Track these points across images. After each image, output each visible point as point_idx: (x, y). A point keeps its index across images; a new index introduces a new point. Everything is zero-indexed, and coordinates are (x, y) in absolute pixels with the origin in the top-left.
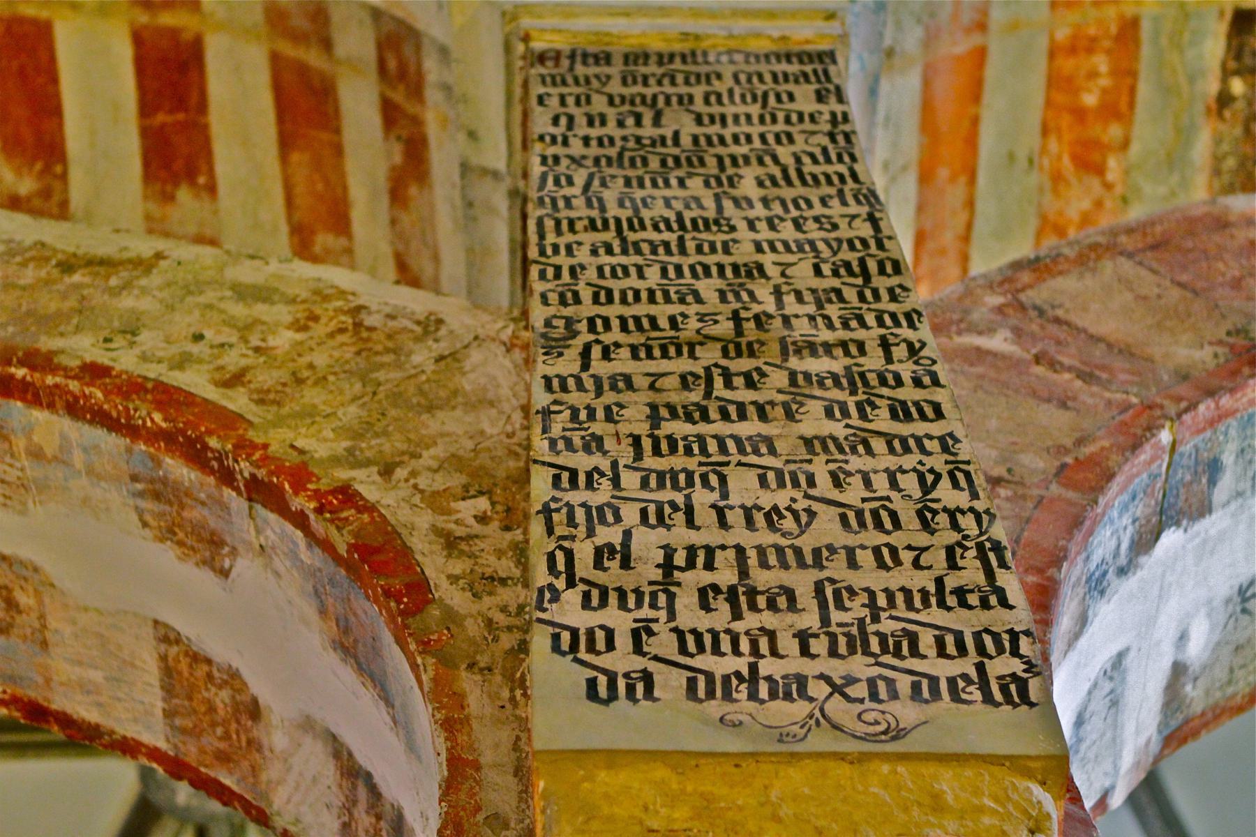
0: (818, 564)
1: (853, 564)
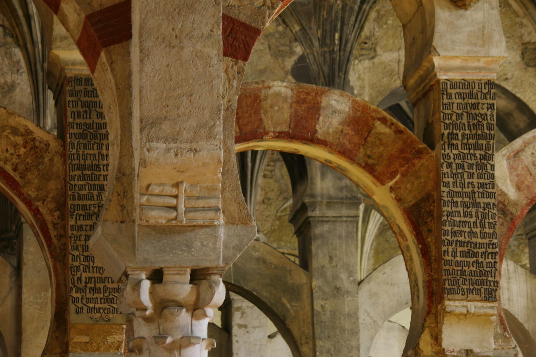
1: (108, 282)
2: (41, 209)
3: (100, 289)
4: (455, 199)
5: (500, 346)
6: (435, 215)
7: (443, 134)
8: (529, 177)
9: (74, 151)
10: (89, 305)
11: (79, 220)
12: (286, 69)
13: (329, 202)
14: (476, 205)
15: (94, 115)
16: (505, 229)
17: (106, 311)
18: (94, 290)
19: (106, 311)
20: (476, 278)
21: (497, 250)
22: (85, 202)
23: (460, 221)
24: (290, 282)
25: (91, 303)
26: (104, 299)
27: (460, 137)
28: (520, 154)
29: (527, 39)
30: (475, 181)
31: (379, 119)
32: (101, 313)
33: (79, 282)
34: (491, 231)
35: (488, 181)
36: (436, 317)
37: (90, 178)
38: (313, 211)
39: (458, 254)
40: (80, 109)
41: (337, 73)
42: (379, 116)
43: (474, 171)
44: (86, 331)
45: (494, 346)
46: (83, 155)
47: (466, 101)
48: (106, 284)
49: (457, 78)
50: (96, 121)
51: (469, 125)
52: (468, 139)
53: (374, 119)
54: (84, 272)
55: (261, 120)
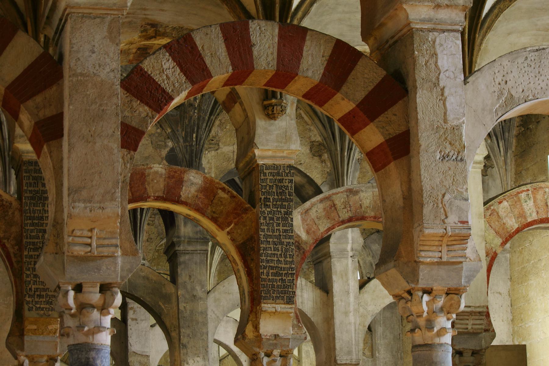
2: (6, 244)
3: (43, 295)
4: (268, 240)
5: (296, 332)
6: (256, 250)
7: (261, 198)
8: (314, 226)
9: (28, 208)
11: (31, 251)
12: (162, 156)
13: (189, 241)
14: (282, 243)
15: (40, 185)
16: (299, 259)
17: (47, 310)
18: (40, 296)
19: (47, 310)
20: (281, 289)
21: (294, 272)
22: (34, 240)
23: (271, 254)
24: (164, 291)
27: (271, 201)
28: (309, 211)
29: (313, 139)
30: (281, 228)
31: (221, 189)
34: (291, 260)
35: (289, 228)
36: (256, 314)
37: (37, 225)
38: (179, 247)
39: (270, 274)
40: (31, 181)
41: (194, 159)
42: (220, 187)
43: (280, 222)
44: (34, 323)
45: (292, 332)
46: (33, 210)
47: (275, 177)
48: (47, 292)
49: (270, 163)
50: (41, 189)
51: (277, 193)
52: (276, 202)
53: (217, 189)
55: (146, 189)
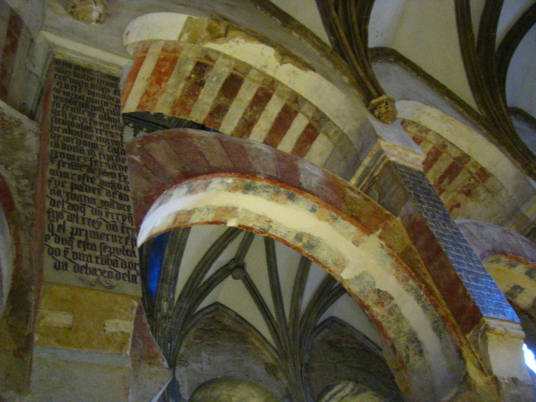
0: (101, 239)
1: (108, 240)
9: (60, 109)
10: (77, 261)
14: (460, 246)
17: (106, 274)
18: (85, 245)
19: (106, 274)
22: (71, 153)
25: (80, 260)
26: (102, 259)
32: (97, 275)
33: (61, 231)
40: (68, 81)
48: (104, 240)
54: (70, 221)
